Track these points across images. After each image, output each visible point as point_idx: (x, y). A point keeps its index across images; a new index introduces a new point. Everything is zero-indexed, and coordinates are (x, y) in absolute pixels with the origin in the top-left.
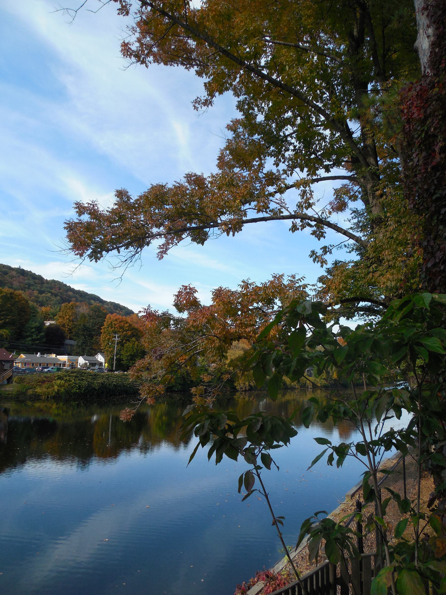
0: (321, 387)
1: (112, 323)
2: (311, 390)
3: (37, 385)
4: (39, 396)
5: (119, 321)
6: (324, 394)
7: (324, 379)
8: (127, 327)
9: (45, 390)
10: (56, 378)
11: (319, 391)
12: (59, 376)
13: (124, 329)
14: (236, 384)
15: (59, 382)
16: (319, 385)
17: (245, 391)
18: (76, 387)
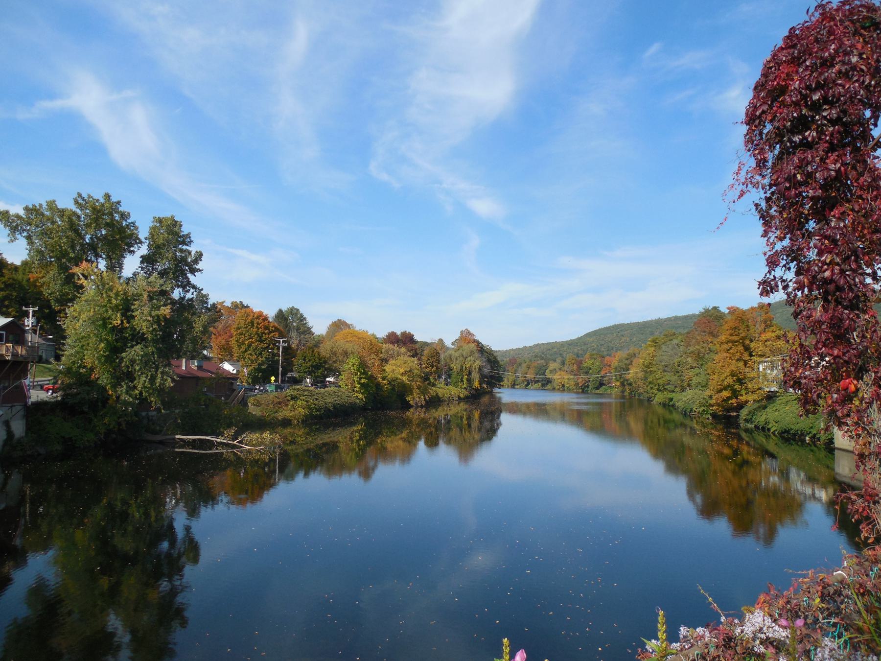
0: (464, 399)
1: (252, 323)
2: (457, 402)
3: (279, 408)
4: (290, 420)
5: (262, 318)
6: (466, 406)
7: (465, 388)
8: (272, 327)
9: (292, 414)
10: (289, 398)
11: (462, 404)
12: (292, 395)
13: (269, 329)
14: (408, 399)
15: (299, 402)
16: (462, 396)
17: (422, 406)
18: (316, 408)
